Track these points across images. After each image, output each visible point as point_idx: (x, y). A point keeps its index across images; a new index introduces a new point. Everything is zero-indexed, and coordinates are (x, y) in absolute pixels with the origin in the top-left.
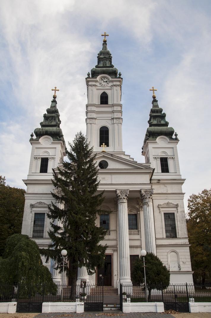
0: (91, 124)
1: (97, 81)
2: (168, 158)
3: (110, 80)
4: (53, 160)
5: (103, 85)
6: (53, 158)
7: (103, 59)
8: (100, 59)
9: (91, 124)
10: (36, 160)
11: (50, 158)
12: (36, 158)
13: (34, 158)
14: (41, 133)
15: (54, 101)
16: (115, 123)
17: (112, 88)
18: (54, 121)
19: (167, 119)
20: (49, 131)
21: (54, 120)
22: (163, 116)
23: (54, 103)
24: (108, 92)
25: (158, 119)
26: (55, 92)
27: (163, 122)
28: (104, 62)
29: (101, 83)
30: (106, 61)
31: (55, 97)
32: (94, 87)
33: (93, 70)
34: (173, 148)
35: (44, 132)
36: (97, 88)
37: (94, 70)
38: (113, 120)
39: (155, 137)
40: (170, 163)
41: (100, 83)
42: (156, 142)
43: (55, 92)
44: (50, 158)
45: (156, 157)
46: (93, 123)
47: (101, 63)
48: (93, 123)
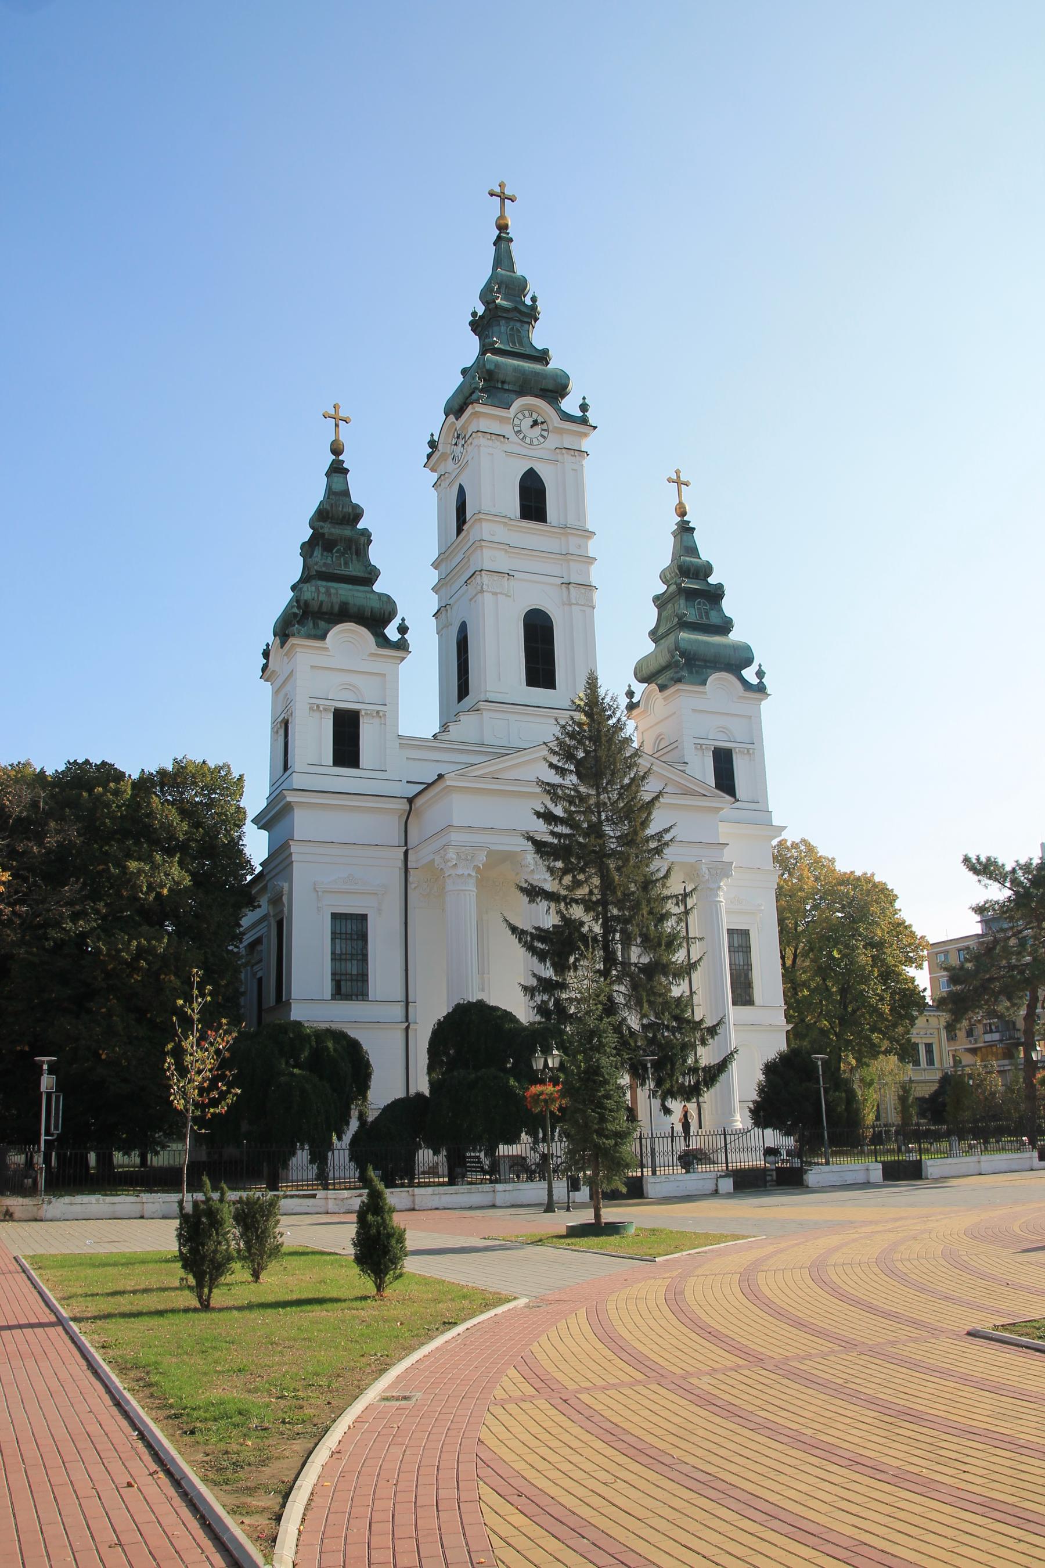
0: (495, 594)
1: (502, 420)
2: (737, 750)
3: (555, 425)
4: (377, 721)
5: (528, 440)
6: (378, 712)
7: (510, 315)
8: (500, 314)
9: (495, 594)
10: (317, 715)
11: (366, 714)
12: (318, 706)
13: (311, 709)
14: (324, 609)
15: (337, 470)
16: (574, 602)
17: (560, 458)
18: (358, 561)
19: (728, 606)
20: (355, 605)
21: (354, 557)
22: (716, 595)
23: (337, 478)
24: (545, 473)
25: (699, 603)
26: (337, 425)
27: (714, 619)
28: (512, 329)
29: (520, 431)
30: (518, 325)
31: (337, 450)
32: (498, 443)
33: (488, 367)
34: (750, 717)
35: (336, 608)
36: (508, 447)
37: (492, 367)
38: (568, 589)
39: (697, 672)
40: (740, 768)
41: (517, 429)
42: (705, 693)
43: (337, 425)
44: (366, 714)
45: (701, 745)
46: (501, 593)
47: (503, 329)
48: (501, 593)
